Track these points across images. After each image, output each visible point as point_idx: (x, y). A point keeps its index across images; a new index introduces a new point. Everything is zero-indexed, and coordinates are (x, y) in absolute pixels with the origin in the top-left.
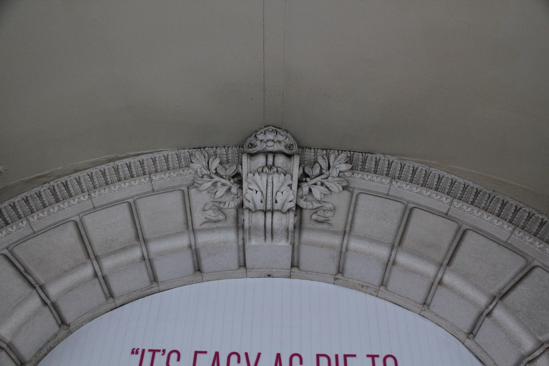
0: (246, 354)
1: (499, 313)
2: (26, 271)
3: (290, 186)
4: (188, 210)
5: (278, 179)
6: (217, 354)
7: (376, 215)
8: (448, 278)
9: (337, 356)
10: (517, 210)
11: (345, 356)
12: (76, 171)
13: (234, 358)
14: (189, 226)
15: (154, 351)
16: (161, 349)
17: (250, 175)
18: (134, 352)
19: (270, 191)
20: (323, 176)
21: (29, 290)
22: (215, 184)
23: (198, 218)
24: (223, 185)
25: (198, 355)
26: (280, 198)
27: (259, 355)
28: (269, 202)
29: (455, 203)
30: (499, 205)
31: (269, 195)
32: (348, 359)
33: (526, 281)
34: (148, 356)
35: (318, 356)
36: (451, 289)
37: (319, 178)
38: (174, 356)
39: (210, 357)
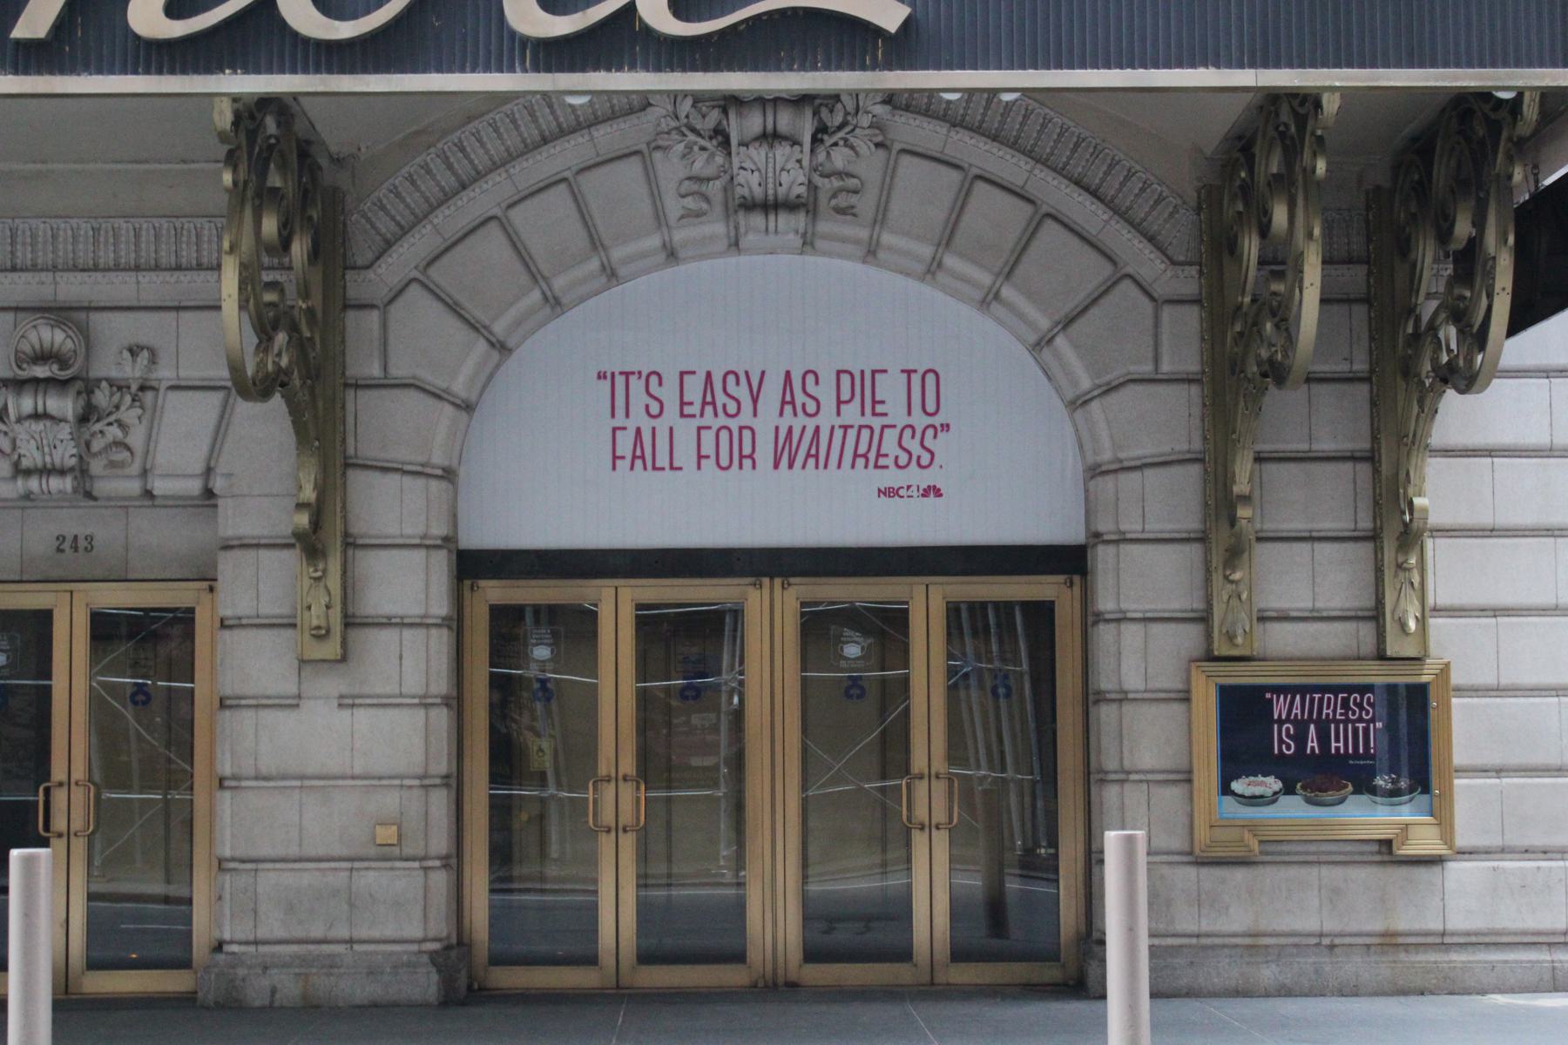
0: (747, 373)
1: (1060, 341)
2: (456, 303)
3: (799, 161)
4: (655, 195)
5: (782, 151)
6: (709, 375)
7: (922, 191)
8: (1007, 292)
9: (862, 372)
10: (1130, 175)
11: (874, 372)
12: (470, 119)
13: (731, 378)
14: (660, 217)
15: (627, 374)
16: (636, 369)
17: (743, 149)
18: (601, 376)
19: (770, 170)
20: (848, 129)
21: (474, 335)
22: (689, 147)
23: (673, 206)
24: (703, 149)
25: (686, 377)
26: (785, 178)
27: (763, 373)
28: (770, 186)
29: (1036, 172)
30: (1104, 168)
31: (770, 174)
32: (878, 376)
33: (1103, 302)
34: (620, 380)
35: (839, 373)
36: (1011, 307)
37: (841, 134)
38: (654, 379)
39: (700, 378)
